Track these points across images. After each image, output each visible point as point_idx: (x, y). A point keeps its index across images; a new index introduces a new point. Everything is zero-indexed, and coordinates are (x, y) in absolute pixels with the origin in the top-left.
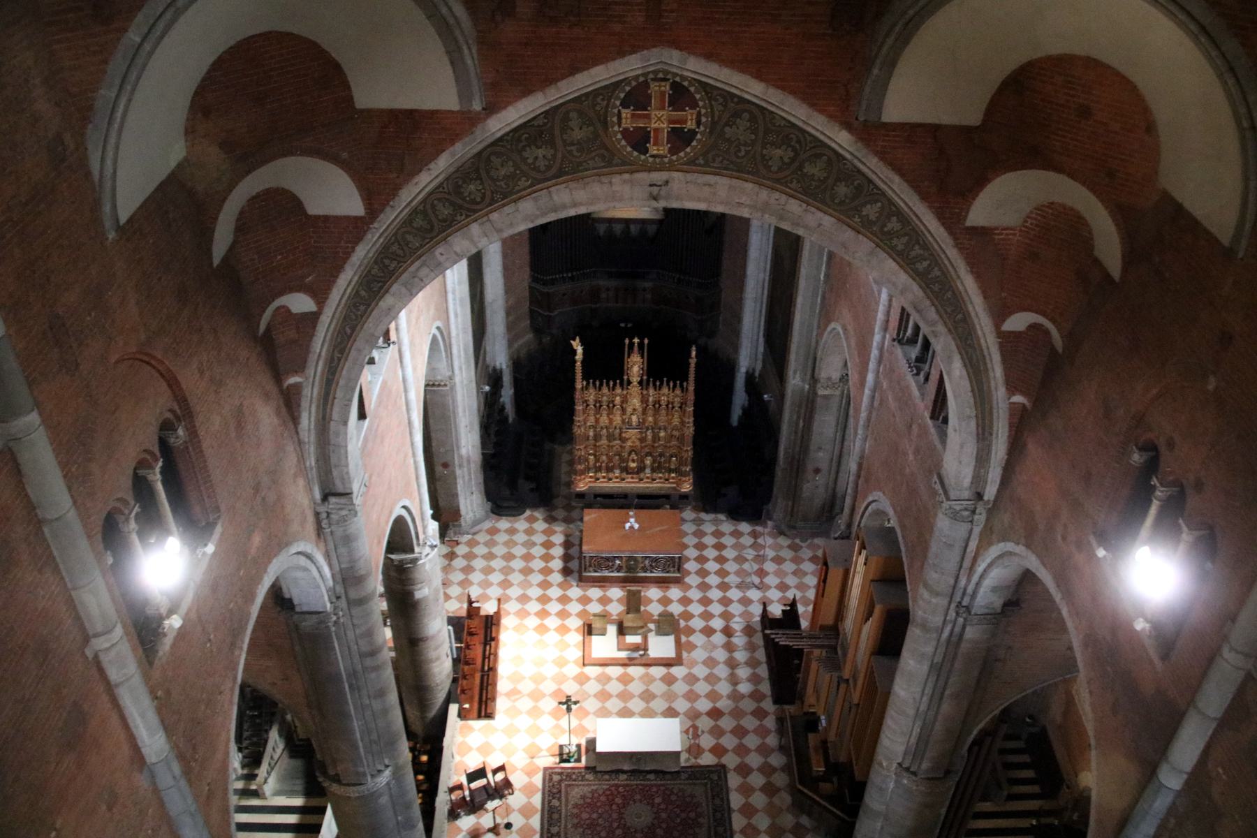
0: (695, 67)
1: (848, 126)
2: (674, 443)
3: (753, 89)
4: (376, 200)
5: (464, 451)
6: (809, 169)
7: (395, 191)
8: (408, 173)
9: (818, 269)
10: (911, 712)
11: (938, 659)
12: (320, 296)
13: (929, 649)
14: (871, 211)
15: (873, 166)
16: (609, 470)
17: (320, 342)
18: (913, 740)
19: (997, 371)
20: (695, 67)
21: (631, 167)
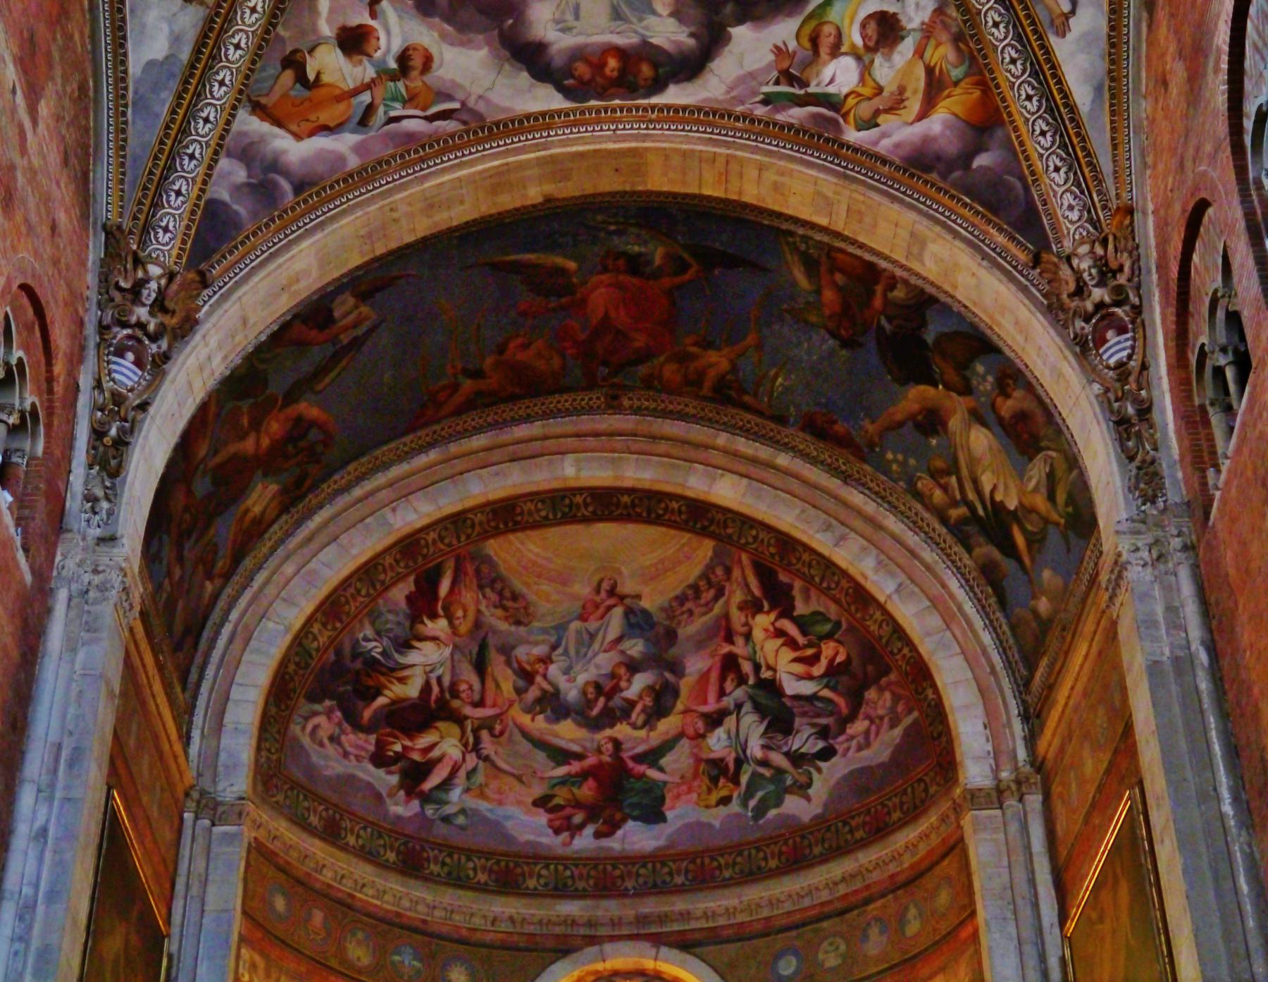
9: (1209, 795)
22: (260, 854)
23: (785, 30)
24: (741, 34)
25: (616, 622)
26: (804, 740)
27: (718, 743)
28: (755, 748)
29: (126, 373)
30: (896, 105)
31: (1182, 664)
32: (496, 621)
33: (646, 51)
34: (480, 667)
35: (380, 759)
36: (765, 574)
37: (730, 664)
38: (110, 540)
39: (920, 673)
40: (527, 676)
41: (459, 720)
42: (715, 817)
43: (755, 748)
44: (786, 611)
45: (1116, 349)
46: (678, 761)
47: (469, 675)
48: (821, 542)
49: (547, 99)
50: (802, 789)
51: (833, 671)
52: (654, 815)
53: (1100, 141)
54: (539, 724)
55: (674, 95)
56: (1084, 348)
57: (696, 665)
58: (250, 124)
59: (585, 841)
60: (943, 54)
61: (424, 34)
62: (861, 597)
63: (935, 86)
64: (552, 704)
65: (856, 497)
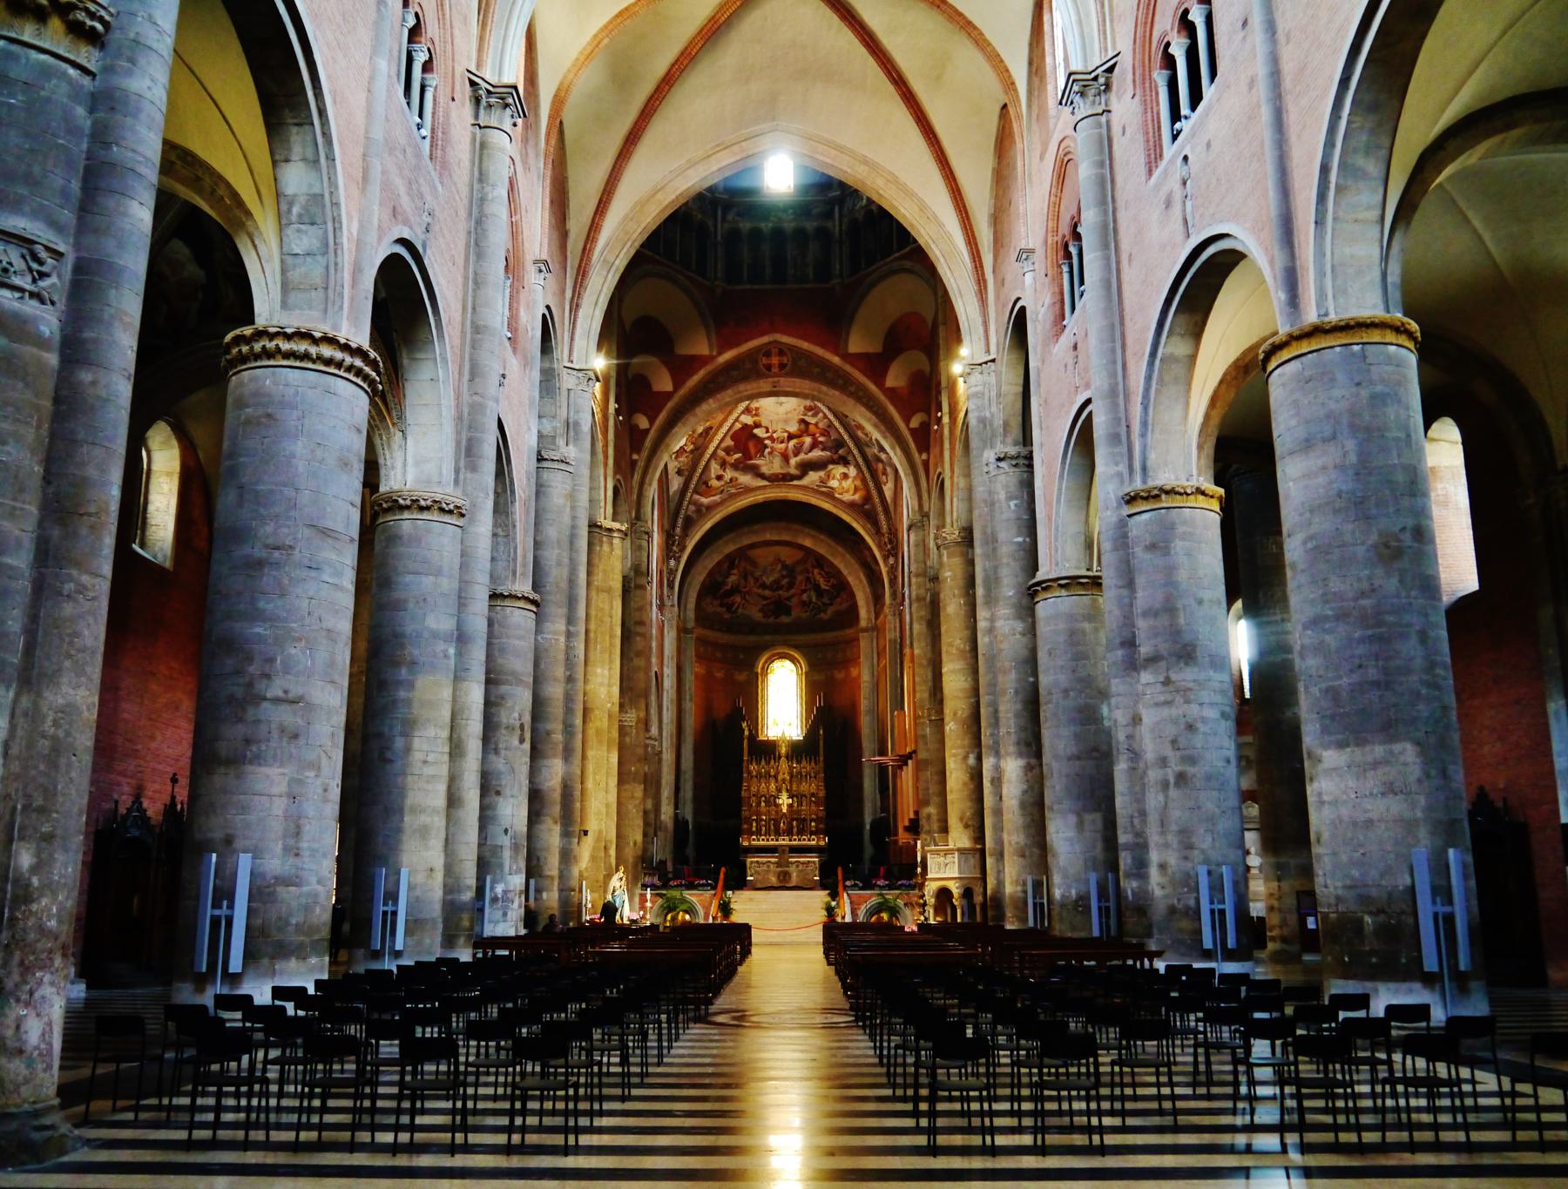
0: (786, 339)
1: (838, 355)
2: (813, 807)
3: (805, 345)
4: (677, 384)
5: (663, 817)
6: (828, 375)
7: (684, 382)
8: (690, 375)
10: (925, 662)
11: (929, 617)
12: (652, 422)
13: (923, 613)
14: (852, 389)
15: (848, 368)
16: (768, 833)
17: (648, 443)
18: (930, 684)
19: (912, 445)
20: (786, 339)
21: (768, 377)
22: (701, 641)
23: (822, 474)
24: (811, 473)
25: (779, 566)
26: (825, 600)
27: (805, 597)
28: (814, 599)
29: (672, 563)
30: (847, 491)
31: (895, 640)
32: (749, 568)
33: (788, 474)
34: (746, 580)
35: (721, 605)
36: (817, 561)
37: (808, 579)
38: (673, 606)
39: (852, 595)
40: (757, 580)
41: (740, 592)
42: (804, 615)
43: (814, 599)
44: (822, 569)
45: (891, 561)
46: (795, 600)
47: (743, 582)
48: (830, 558)
49: (765, 483)
50: (825, 611)
51: (833, 585)
52: (788, 611)
53: (892, 509)
54: (760, 591)
55: (795, 483)
56: (886, 558)
57: (800, 578)
58: (696, 497)
59: (771, 620)
60: (858, 483)
61: (736, 474)
62: (839, 572)
63: (856, 490)
64: (764, 586)
65: (840, 549)
